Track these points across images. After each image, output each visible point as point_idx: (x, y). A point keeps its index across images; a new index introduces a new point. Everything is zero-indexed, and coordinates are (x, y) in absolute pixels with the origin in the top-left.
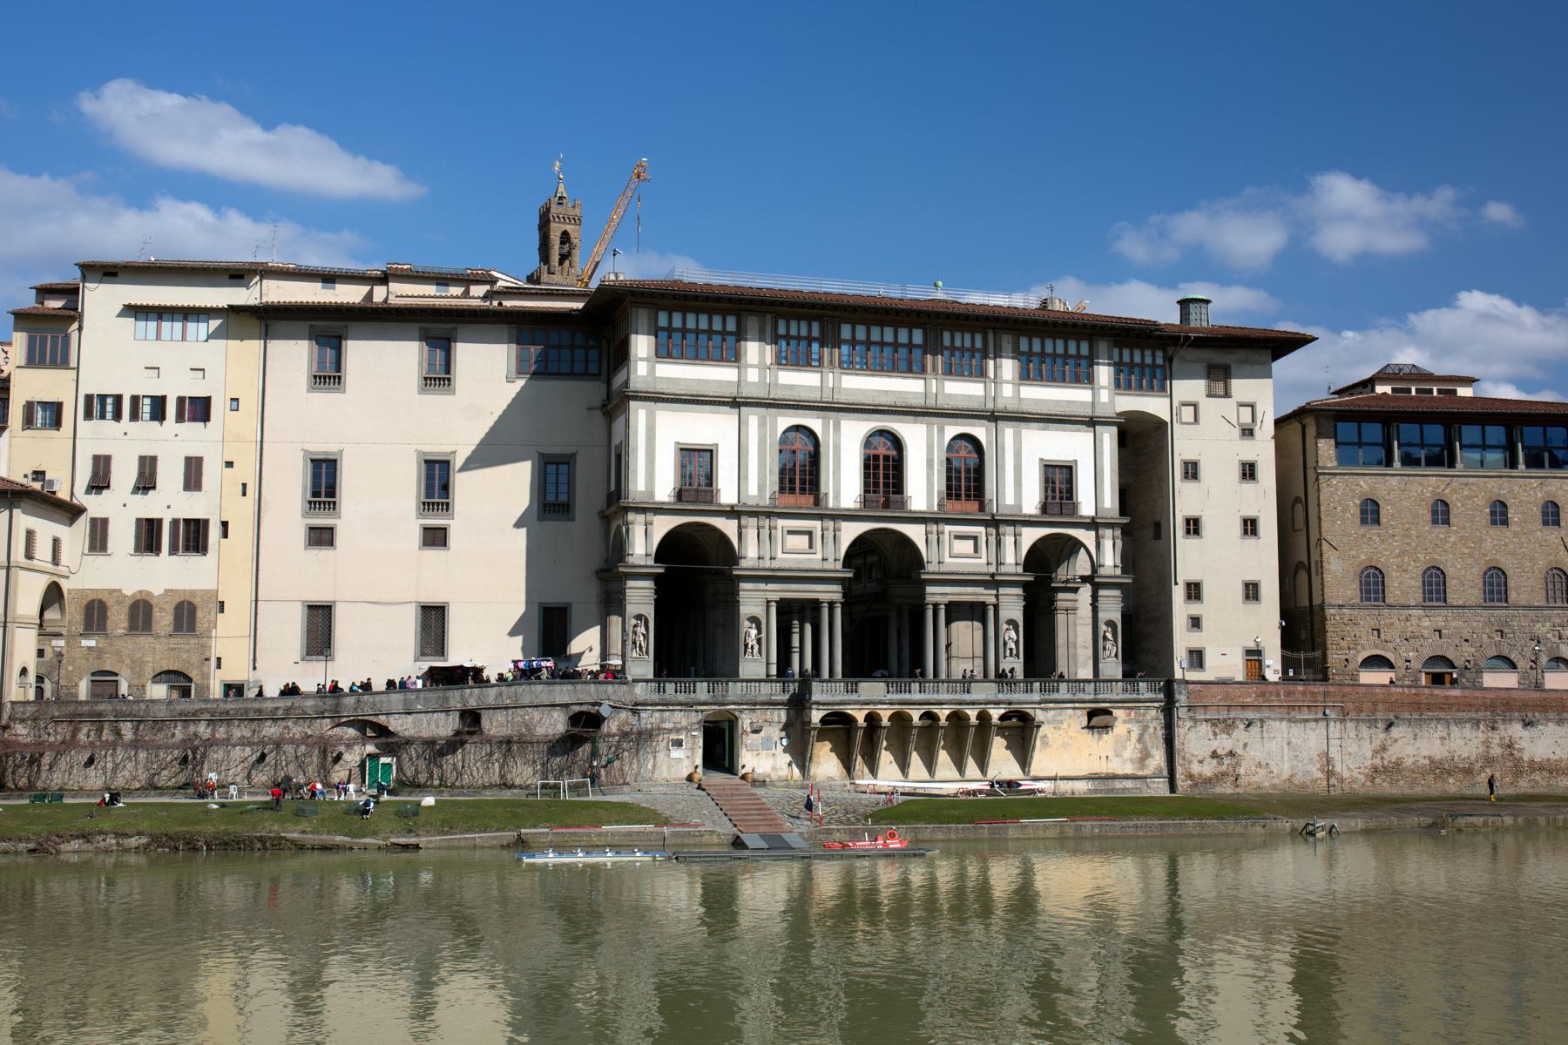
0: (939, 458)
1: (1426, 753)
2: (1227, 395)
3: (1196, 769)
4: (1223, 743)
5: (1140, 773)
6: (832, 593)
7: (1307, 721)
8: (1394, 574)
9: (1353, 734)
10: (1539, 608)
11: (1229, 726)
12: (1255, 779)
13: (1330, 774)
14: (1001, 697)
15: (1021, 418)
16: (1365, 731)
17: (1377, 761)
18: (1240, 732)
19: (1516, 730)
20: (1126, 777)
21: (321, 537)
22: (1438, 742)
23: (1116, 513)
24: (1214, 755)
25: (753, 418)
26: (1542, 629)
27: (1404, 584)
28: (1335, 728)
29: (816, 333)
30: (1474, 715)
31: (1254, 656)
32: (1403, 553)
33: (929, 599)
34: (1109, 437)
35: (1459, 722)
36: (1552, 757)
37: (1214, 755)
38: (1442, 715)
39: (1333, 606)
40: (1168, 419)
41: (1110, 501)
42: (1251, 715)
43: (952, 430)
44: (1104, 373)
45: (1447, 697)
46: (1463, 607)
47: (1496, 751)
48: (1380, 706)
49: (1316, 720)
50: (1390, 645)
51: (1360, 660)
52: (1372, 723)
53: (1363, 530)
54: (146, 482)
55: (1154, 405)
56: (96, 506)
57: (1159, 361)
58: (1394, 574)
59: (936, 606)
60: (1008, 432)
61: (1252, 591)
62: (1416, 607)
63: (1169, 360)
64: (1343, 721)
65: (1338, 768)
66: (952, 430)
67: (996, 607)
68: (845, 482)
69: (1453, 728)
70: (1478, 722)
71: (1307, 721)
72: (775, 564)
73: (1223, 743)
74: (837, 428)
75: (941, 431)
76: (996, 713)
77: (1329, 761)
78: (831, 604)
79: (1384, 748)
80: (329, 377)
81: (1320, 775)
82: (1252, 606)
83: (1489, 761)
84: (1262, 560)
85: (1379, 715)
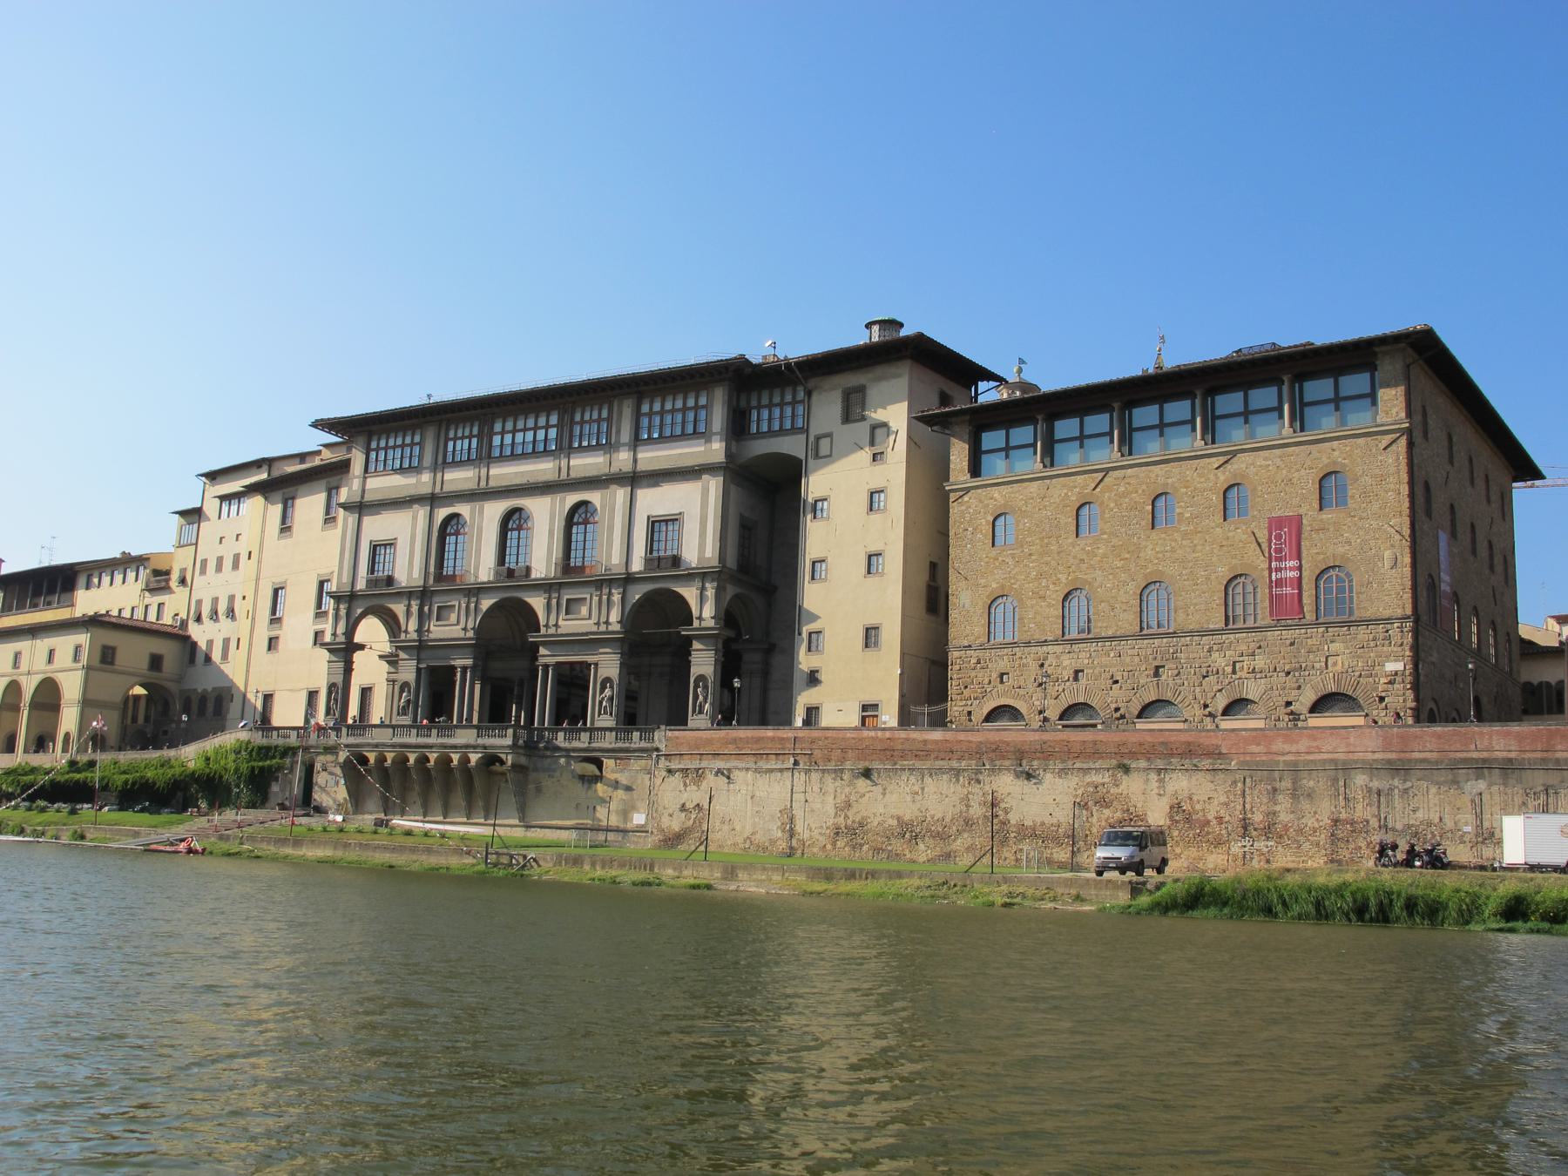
0: (559, 524)
1: (895, 812)
2: (863, 418)
3: (665, 822)
4: (694, 795)
5: (622, 826)
6: (462, 661)
7: (772, 771)
8: (1029, 603)
9: (816, 789)
10: (1213, 633)
11: (699, 774)
12: (719, 835)
13: (792, 833)
14: (480, 741)
15: (635, 479)
16: (830, 784)
17: (841, 820)
18: (710, 780)
19: (1006, 784)
20: (608, 830)
21: (272, 643)
22: (909, 798)
23: (715, 563)
24: (683, 808)
25: (422, 512)
26: (1220, 661)
27: (1042, 616)
28: (800, 778)
29: (475, 431)
30: (955, 764)
31: (869, 709)
32: (1041, 575)
33: (542, 661)
34: (714, 484)
35: (933, 772)
36: (1048, 820)
37: (683, 808)
38: (918, 764)
39: (960, 648)
40: (803, 457)
41: (711, 552)
42: (719, 764)
43: (572, 498)
44: (718, 418)
45: (925, 742)
46: (1111, 638)
47: (977, 811)
48: (850, 754)
49: (781, 770)
50: (1022, 692)
51: (985, 711)
52: (838, 773)
53: (994, 553)
54: (214, 615)
55: (792, 446)
56: (195, 631)
57: (801, 395)
58: (1029, 603)
59: (546, 667)
60: (621, 494)
61: (871, 636)
62: (1056, 642)
63: (809, 394)
64: (807, 771)
65: (799, 828)
66: (572, 498)
67: (596, 665)
68: (480, 562)
69: (928, 780)
70: (957, 773)
71: (772, 771)
72: (432, 636)
73: (694, 795)
74: (481, 512)
75: (563, 501)
76: (474, 758)
77: (792, 820)
78: (464, 669)
79: (849, 805)
80: (285, 528)
81: (780, 834)
82: (870, 653)
83: (968, 823)
84: (887, 601)
85: (848, 765)
